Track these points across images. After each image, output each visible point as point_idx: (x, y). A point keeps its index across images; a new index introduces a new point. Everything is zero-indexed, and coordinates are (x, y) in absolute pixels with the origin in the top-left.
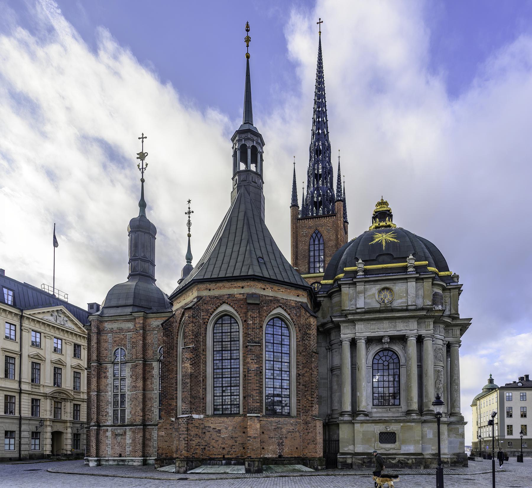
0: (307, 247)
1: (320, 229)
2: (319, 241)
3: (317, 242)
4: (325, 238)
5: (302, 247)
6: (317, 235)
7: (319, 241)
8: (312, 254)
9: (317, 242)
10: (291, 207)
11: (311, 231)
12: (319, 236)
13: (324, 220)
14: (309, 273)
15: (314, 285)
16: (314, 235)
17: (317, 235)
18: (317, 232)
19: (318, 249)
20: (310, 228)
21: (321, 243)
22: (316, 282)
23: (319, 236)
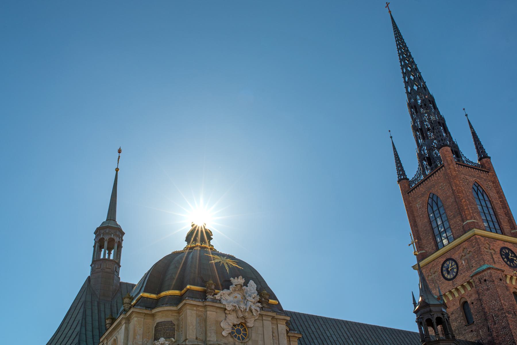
0: (426, 220)
1: (433, 191)
2: (437, 204)
3: (435, 208)
4: (441, 198)
5: (422, 222)
6: (433, 200)
7: (437, 204)
8: (434, 225)
9: (435, 208)
10: (399, 181)
11: (426, 198)
12: (435, 199)
13: (434, 178)
14: (438, 249)
15: (445, 265)
16: (430, 201)
17: (433, 200)
18: (431, 196)
19: (439, 215)
20: (423, 195)
21: (439, 206)
22: (447, 260)
23: (435, 199)
